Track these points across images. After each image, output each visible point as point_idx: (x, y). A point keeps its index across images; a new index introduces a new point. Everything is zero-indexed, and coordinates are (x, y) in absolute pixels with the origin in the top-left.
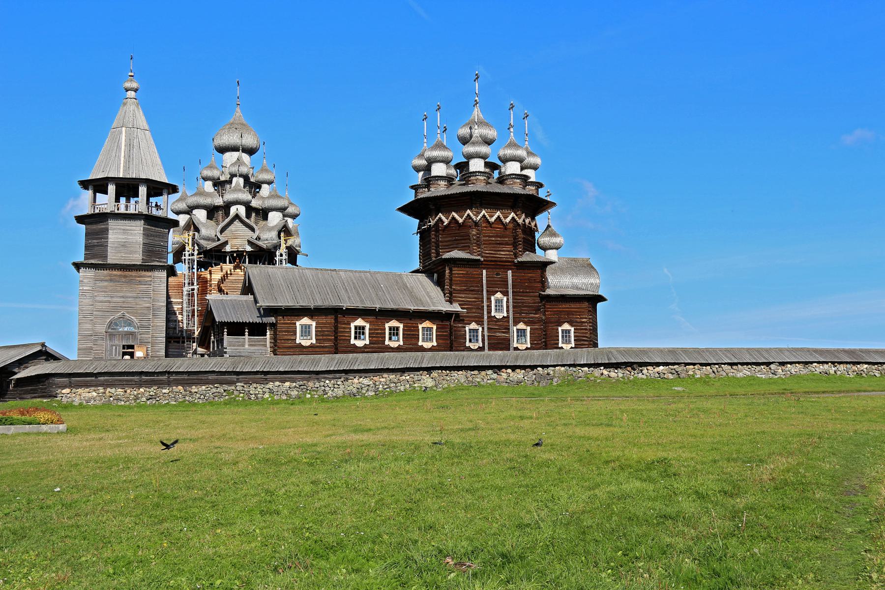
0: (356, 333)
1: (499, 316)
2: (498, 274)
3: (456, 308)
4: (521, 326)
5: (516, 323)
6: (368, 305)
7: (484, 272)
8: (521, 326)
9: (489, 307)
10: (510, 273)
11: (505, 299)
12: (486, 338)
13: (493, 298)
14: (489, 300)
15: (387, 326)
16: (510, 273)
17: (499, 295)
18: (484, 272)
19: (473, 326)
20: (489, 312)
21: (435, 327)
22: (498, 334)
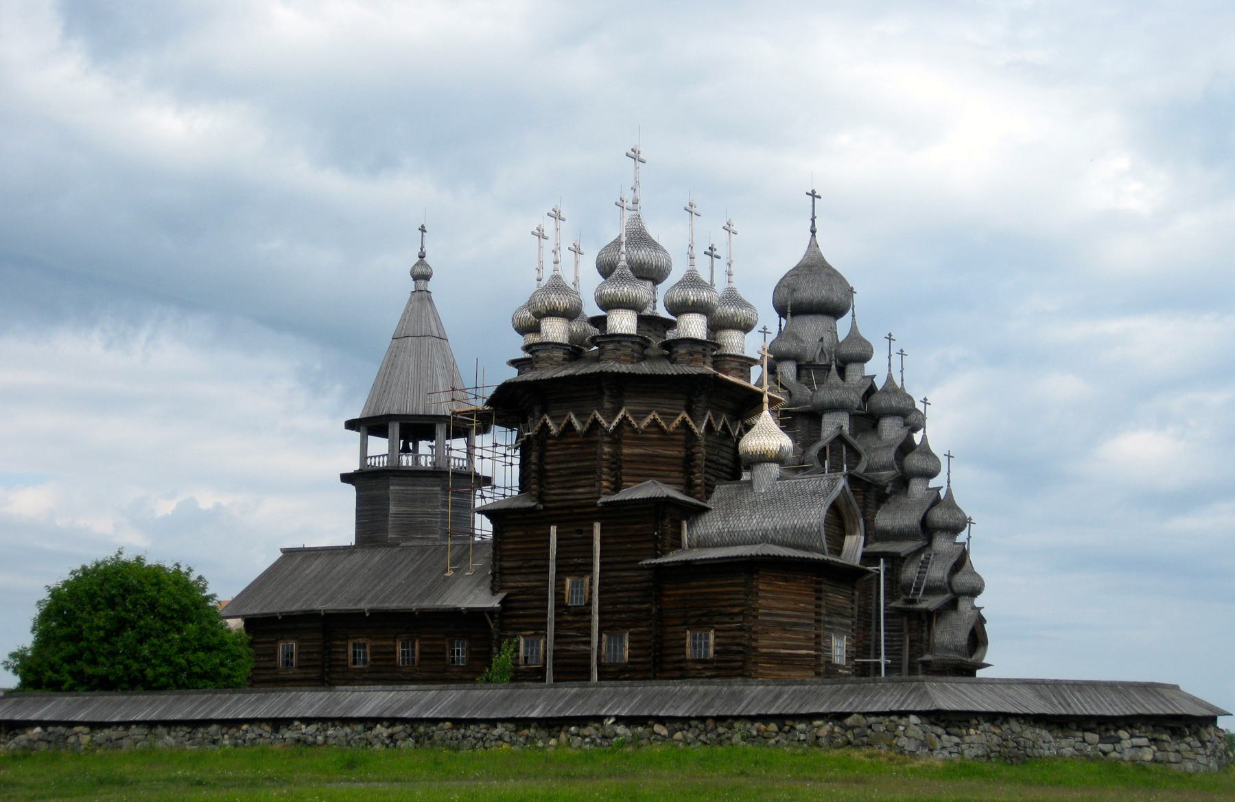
0: (355, 653)
2: (581, 532)
3: (494, 603)
7: (553, 529)
10: (597, 527)
12: (550, 654)
16: (597, 527)
18: (553, 529)
22: (572, 647)
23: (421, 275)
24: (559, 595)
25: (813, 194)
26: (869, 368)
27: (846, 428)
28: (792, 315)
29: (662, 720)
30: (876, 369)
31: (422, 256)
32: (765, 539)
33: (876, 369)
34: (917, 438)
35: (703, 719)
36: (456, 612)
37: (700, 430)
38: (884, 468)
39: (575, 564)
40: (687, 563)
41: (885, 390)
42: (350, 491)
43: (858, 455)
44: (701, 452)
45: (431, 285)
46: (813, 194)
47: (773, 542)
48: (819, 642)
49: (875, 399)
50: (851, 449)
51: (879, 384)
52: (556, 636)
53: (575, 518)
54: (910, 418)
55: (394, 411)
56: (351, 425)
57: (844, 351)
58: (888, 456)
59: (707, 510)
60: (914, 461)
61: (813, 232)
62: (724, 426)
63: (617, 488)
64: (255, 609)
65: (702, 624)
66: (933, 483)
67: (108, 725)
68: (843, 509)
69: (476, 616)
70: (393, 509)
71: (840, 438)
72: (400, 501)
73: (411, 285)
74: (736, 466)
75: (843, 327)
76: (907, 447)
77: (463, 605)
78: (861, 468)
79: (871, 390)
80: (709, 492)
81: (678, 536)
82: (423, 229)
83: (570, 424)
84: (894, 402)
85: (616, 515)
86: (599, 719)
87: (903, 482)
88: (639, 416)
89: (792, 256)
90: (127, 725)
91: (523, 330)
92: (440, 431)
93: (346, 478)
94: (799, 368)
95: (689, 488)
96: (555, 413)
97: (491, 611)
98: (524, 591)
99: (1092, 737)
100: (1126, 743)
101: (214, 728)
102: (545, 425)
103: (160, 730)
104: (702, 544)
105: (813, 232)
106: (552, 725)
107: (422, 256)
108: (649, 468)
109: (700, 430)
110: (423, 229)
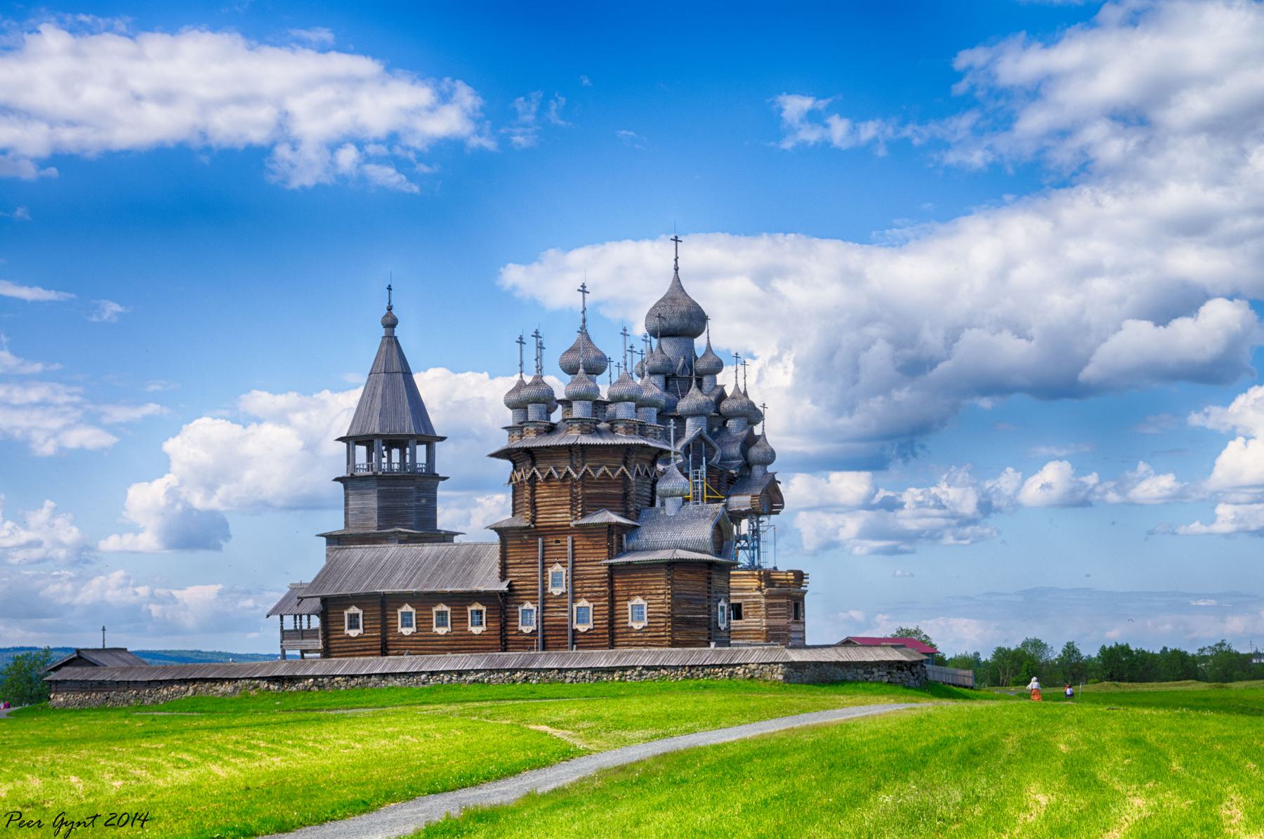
1: (557, 591)
3: (503, 587)
4: (583, 603)
5: (574, 600)
6: (412, 589)
8: (583, 603)
9: (544, 582)
10: (569, 538)
11: (564, 571)
13: (550, 571)
14: (544, 572)
15: (434, 610)
17: (558, 567)
19: (528, 605)
20: (544, 589)
21: (484, 609)
23: (390, 323)
26: (720, 379)
27: (705, 429)
28: (662, 336)
29: (664, 667)
30: (726, 380)
31: (390, 309)
33: (726, 380)
34: (757, 430)
35: (684, 667)
36: (478, 592)
38: (733, 458)
40: (629, 563)
41: (733, 397)
42: (340, 485)
43: (714, 450)
44: (633, 490)
45: (398, 332)
47: (681, 548)
49: (725, 405)
50: (708, 444)
51: (729, 391)
52: (544, 608)
54: (752, 415)
55: (377, 431)
56: (341, 439)
57: (701, 365)
58: (735, 450)
60: (755, 452)
61: (677, 269)
62: (647, 473)
63: (583, 516)
64: (329, 592)
66: (770, 469)
67: (358, 676)
68: (722, 526)
71: (700, 437)
73: (382, 332)
75: (700, 343)
76: (751, 441)
77: (482, 589)
78: (716, 459)
79: (722, 396)
80: (638, 513)
81: (620, 545)
82: (389, 288)
83: (551, 473)
86: (634, 667)
87: (747, 466)
88: (595, 469)
89: (660, 289)
90: (369, 676)
91: (512, 406)
92: (411, 442)
94: (667, 379)
96: (540, 466)
97: (501, 593)
99: (861, 671)
100: (876, 674)
101: (423, 676)
102: (534, 474)
103: (391, 678)
105: (677, 269)
107: (390, 309)
110: (389, 288)
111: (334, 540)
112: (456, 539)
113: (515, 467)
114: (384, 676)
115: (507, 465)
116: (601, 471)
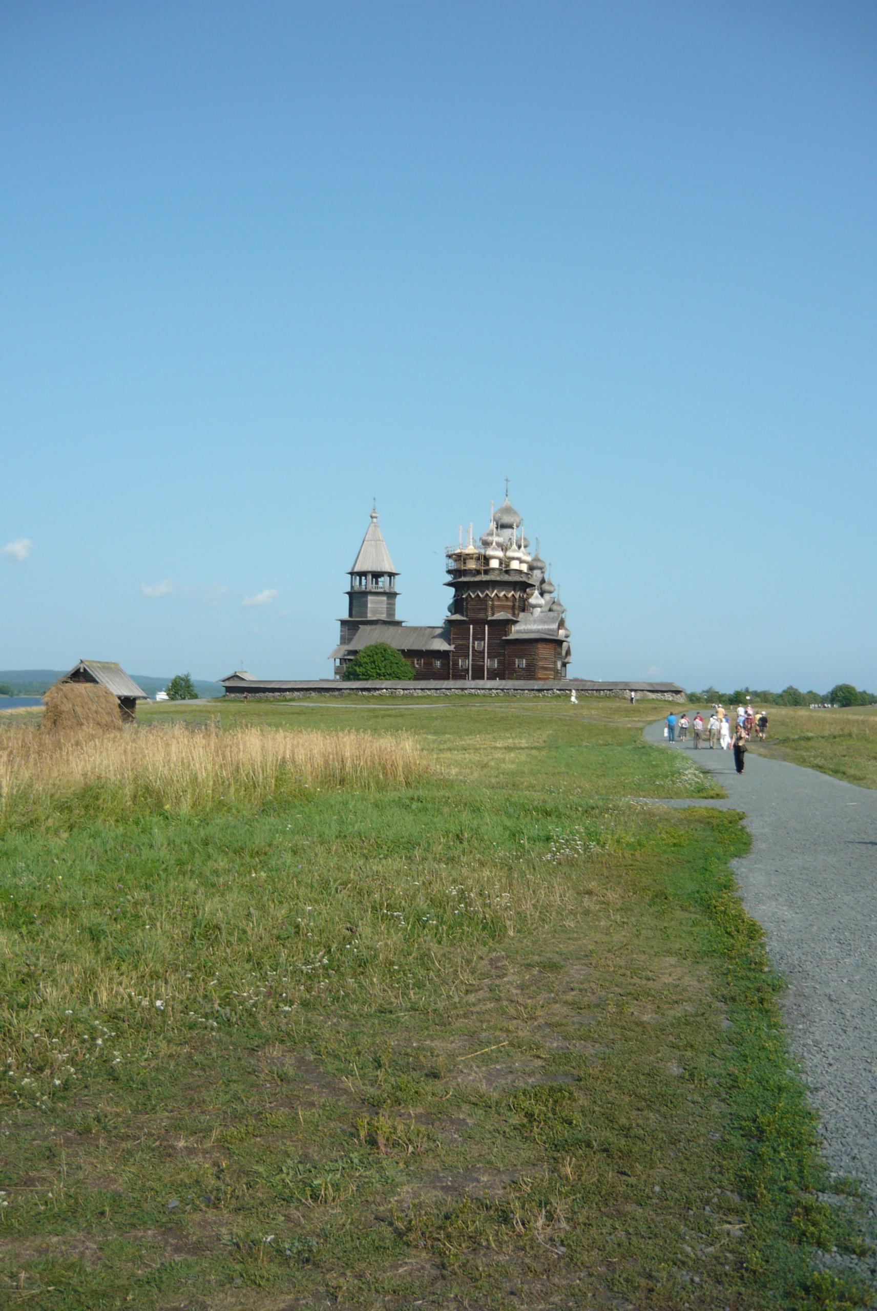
3: (451, 648)
14: (474, 643)
24: (473, 647)
25: (507, 480)
32: (538, 631)
37: (517, 597)
39: (479, 637)
42: (347, 596)
44: (517, 604)
46: (507, 480)
48: (555, 663)
53: (480, 623)
55: (370, 569)
59: (517, 622)
65: (521, 657)
66: (552, 595)
69: (446, 653)
70: (369, 605)
72: (372, 603)
74: (524, 607)
84: (539, 564)
85: (494, 624)
93: (347, 593)
95: (514, 614)
98: (462, 645)
104: (518, 632)
106: (539, 690)
108: (503, 608)
109: (517, 597)
111: (343, 623)
112: (403, 624)
113: (456, 591)
114: (422, 689)
115: (452, 591)
116: (502, 594)
